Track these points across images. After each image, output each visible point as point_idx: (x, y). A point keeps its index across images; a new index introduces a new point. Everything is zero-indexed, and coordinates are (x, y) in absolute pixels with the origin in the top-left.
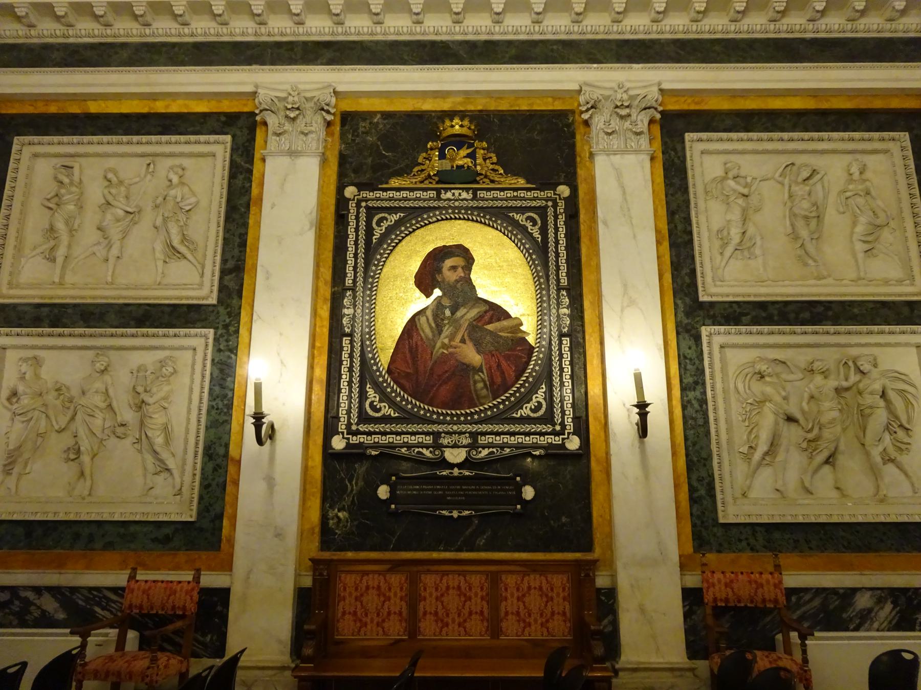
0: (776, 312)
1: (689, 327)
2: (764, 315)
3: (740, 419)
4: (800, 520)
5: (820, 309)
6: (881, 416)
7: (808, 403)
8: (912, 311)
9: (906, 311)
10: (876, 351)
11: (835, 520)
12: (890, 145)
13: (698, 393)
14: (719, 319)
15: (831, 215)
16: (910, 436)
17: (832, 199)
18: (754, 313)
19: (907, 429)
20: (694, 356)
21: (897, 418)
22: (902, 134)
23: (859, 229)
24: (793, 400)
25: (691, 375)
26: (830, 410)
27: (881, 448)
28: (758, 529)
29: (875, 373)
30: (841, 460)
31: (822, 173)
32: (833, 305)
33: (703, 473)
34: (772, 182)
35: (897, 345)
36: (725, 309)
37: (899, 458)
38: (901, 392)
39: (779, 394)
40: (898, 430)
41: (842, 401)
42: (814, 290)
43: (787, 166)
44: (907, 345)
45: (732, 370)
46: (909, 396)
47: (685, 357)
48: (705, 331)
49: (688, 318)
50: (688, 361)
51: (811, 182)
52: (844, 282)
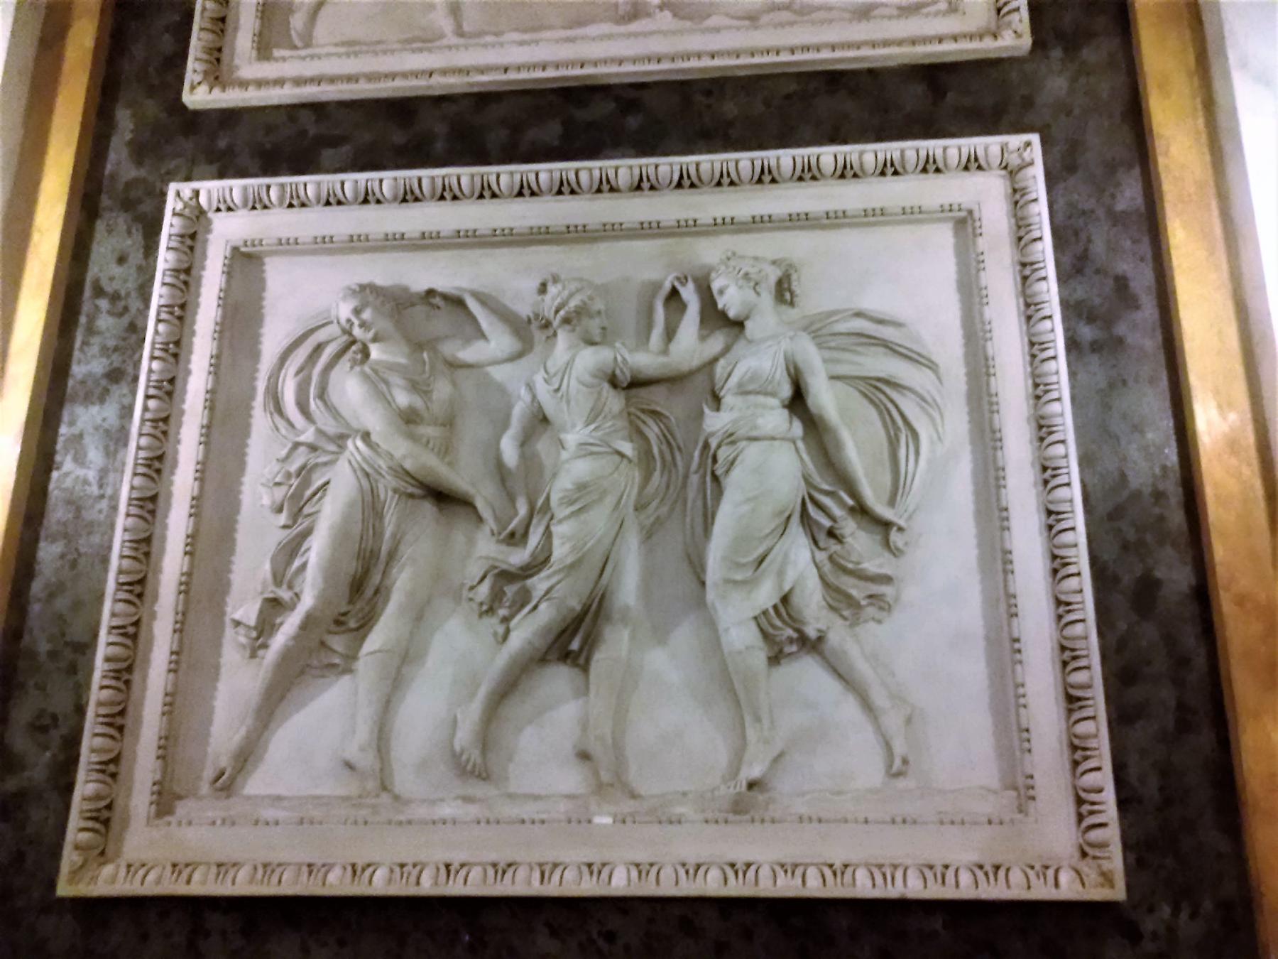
0: (441, 129)
1: (134, 194)
2: (399, 138)
3: (266, 501)
4: (380, 884)
5: (602, 109)
6: (769, 468)
7: (526, 441)
10: (797, 245)
11: (523, 885)
13: (107, 413)
16: (895, 552)
18: (367, 137)
19: (886, 525)
20: (131, 285)
21: (846, 482)
24: (473, 430)
25: (105, 351)
26: (585, 453)
27: (765, 595)
28: (215, 921)
29: (766, 319)
30: (616, 645)
33: (60, 702)
35: (874, 217)
36: (269, 129)
37: (839, 635)
38: (878, 390)
39: (387, 400)
40: (849, 526)
41: (652, 430)
44: (912, 215)
45: (273, 339)
46: (909, 406)
47: (99, 291)
48: (177, 194)
50: (104, 304)
52: (713, 21)
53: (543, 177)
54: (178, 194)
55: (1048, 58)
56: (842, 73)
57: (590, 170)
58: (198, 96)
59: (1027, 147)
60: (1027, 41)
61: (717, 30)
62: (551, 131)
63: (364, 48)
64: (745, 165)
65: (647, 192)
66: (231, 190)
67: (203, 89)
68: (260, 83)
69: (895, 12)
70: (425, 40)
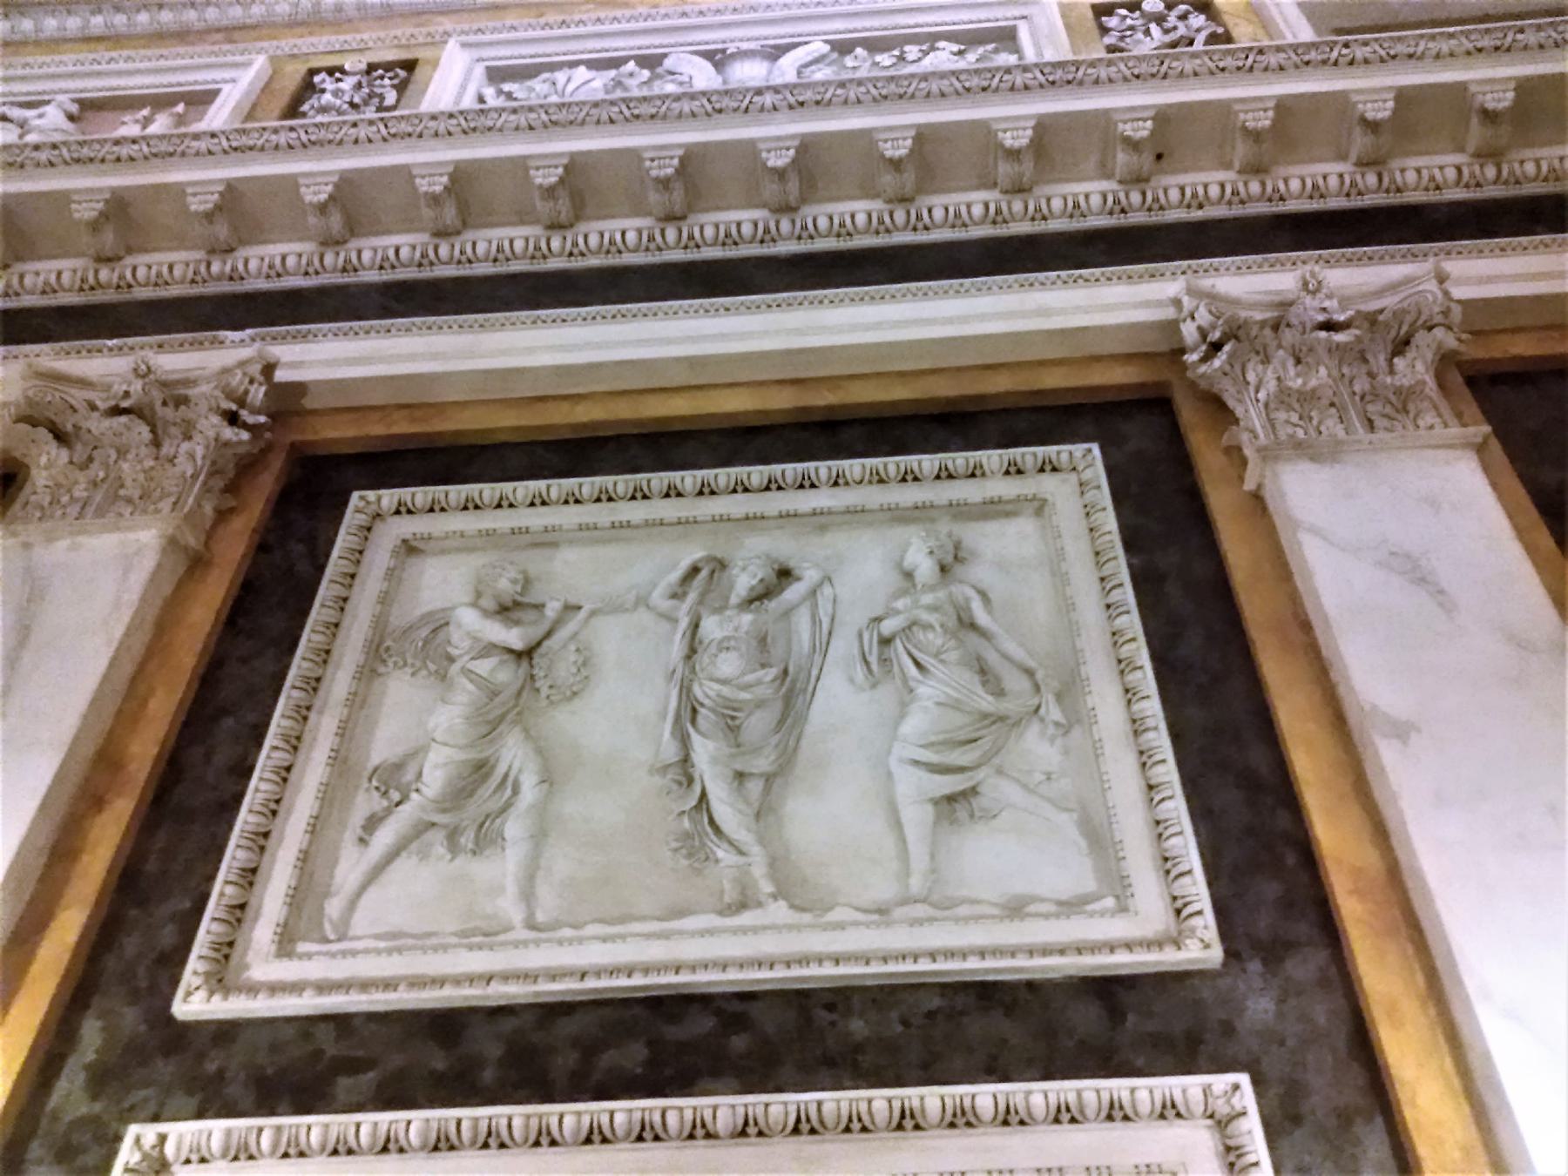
2: (439, 1062)
5: (701, 1025)
8: (1115, 1014)
9: (1086, 1018)
12: (1048, 485)
14: (234, 1090)
15: (839, 698)
17: (843, 646)
18: (396, 1060)
22: (1078, 449)
23: (916, 724)
31: (810, 576)
32: (755, 1009)
34: (644, 617)
42: (656, 951)
43: (695, 570)
49: (95, 1097)
51: (772, 605)
52: (833, 916)
53: (619, 1118)
54: (138, 1140)
55: (1244, 971)
56: (995, 985)
57: (681, 1109)
58: (193, 1003)
59: (1235, 1089)
60: (1216, 955)
61: (841, 926)
62: (633, 1055)
63: (410, 942)
64: (880, 1106)
65: (753, 1140)
66: (210, 1135)
67: (201, 995)
68: (275, 988)
69: (1053, 908)
70: (486, 934)
